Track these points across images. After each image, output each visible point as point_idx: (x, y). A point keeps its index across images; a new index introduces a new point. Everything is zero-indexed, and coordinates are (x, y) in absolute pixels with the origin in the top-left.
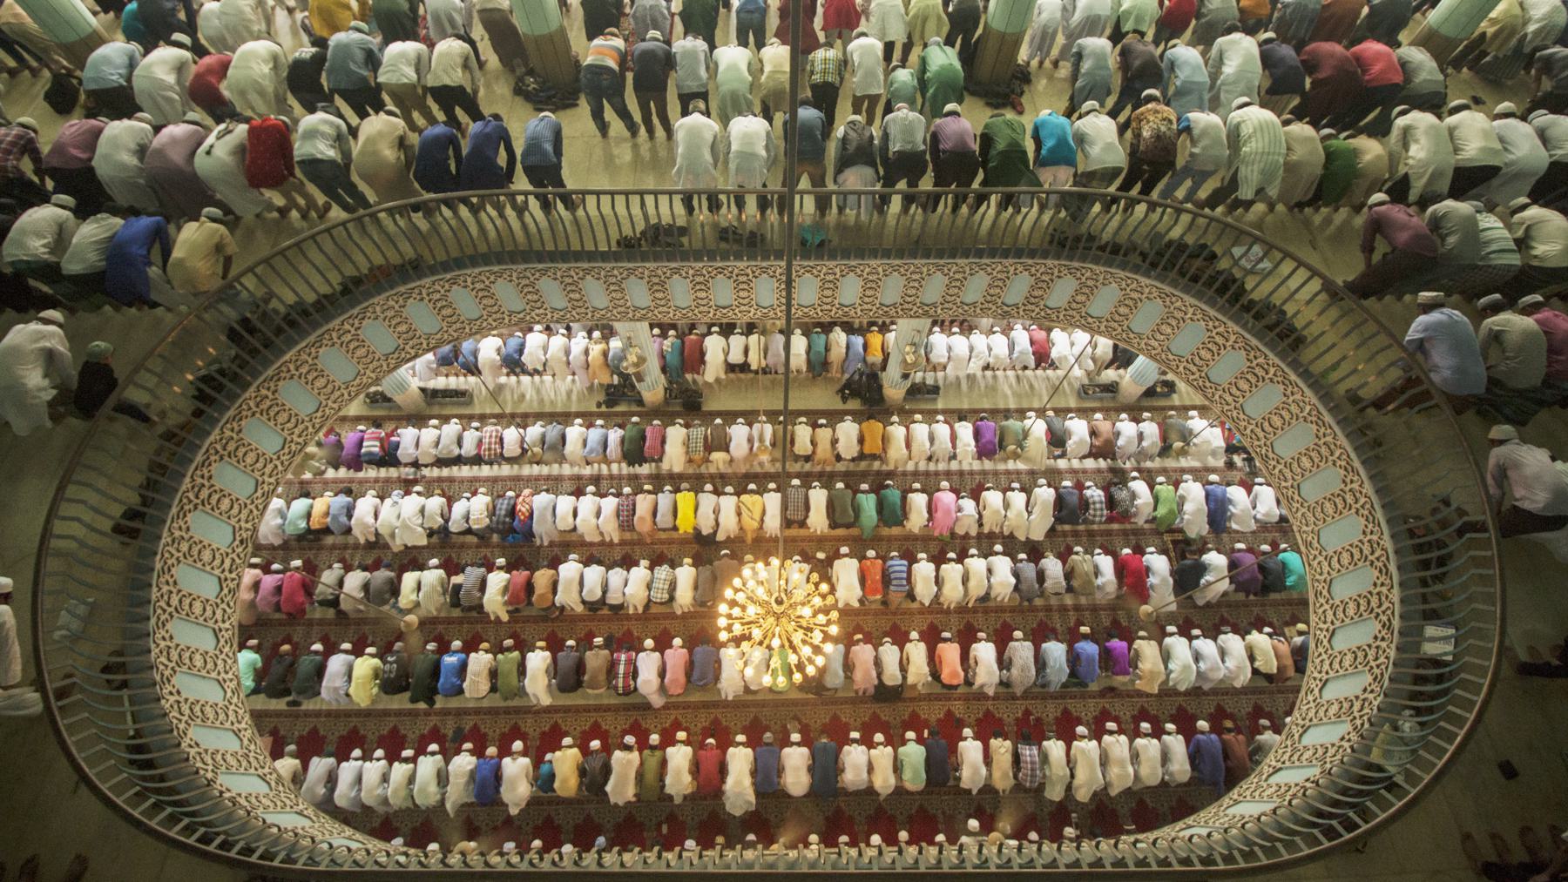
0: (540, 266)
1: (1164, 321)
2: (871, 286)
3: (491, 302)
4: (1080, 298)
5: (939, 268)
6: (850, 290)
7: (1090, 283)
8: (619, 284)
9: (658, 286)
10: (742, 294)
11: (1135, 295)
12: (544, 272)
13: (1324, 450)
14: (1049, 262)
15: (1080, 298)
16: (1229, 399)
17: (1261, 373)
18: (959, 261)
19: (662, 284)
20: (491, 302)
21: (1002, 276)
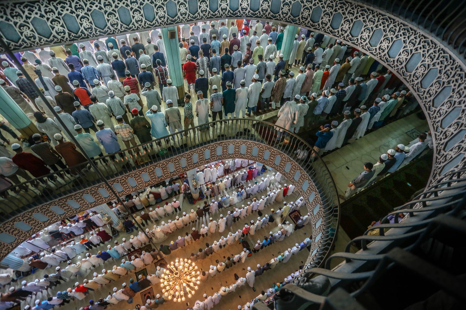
0: (48, 203)
1: (248, 149)
2: (164, 168)
3: (34, 222)
4: (225, 150)
5: (182, 156)
6: (159, 172)
7: (225, 146)
8: (80, 198)
9: (95, 194)
10: (124, 186)
11: (237, 145)
12: (50, 204)
13: (294, 167)
14: (211, 144)
15: (225, 150)
16: (271, 163)
17: (274, 154)
18: (187, 152)
19: (96, 192)
20: (34, 222)
21: (201, 152)
